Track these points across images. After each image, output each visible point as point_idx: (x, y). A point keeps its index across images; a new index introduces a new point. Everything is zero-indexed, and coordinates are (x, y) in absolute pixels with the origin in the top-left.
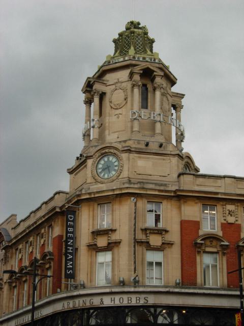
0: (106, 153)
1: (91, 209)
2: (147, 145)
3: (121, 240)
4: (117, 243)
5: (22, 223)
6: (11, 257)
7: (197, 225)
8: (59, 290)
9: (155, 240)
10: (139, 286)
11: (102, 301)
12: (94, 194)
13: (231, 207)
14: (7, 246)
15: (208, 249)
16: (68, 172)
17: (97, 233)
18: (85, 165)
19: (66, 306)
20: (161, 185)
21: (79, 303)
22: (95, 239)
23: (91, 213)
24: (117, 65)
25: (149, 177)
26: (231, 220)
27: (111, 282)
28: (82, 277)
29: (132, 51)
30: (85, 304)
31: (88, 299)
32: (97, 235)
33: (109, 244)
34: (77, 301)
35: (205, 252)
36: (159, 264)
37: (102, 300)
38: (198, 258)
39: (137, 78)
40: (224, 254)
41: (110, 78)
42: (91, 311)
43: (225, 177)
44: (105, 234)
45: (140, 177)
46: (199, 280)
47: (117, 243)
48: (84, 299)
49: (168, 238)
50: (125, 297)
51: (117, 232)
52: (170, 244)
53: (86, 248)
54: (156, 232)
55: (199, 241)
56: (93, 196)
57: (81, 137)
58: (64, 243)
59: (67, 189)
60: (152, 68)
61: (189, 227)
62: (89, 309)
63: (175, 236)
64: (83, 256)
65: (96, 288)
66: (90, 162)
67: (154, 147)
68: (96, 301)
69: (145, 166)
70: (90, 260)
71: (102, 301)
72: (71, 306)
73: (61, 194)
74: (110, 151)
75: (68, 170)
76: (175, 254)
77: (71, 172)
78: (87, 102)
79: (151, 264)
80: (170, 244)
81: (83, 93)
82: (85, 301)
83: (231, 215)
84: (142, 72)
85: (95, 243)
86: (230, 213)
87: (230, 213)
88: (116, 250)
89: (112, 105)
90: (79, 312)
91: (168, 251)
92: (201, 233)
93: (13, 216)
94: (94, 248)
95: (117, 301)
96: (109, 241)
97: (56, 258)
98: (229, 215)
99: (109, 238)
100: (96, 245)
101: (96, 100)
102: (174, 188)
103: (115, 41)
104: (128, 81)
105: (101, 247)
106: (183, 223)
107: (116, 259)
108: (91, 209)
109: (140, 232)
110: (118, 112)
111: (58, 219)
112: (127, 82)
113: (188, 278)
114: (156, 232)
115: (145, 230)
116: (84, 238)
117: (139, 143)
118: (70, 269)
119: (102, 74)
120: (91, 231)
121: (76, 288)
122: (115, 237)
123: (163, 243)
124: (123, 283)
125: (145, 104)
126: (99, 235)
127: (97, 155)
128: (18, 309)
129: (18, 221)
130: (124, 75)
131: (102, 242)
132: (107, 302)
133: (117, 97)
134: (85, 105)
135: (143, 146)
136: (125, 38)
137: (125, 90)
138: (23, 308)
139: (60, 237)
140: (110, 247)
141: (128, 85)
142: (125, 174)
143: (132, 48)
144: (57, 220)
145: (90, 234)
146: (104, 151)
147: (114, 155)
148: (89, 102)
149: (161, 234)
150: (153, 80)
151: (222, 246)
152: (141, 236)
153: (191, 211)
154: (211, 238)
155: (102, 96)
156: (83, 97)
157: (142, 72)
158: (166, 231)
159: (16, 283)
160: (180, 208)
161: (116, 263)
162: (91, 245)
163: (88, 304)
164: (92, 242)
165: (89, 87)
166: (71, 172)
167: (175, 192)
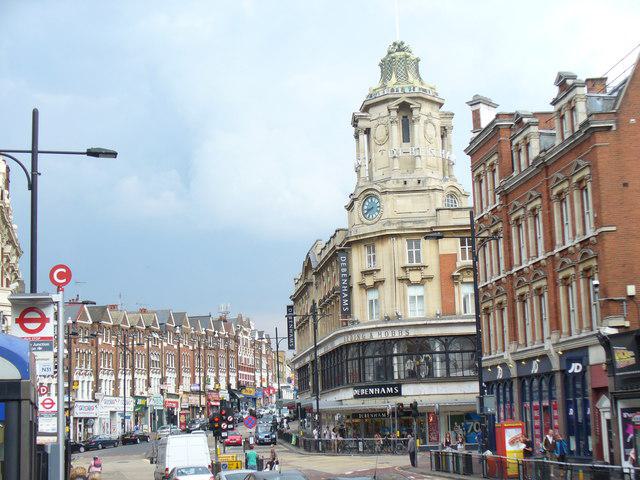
2: (405, 183)
4: (382, 282)
9: (415, 276)
10: (400, 321)
15: (465, 280)
17: (365, 273)
20: (420, 222)
21: (355, 338)
25: (409, 215)
28: (357, 314)
29: (394, 80)
36: (421, 297)
41: (374, 112)
46: (459, 308)
47: (382, 282)
49: (427, 272)
50: (390, 332)
52: (430, 278)
55: (455, 274)
59: (346, 226)
63: (433, 270)
64: (356, 291)
66: (356, 203)
67: (412, 185)
68: (367, 337)
76: (433, 287)
79: (413, 298)
80: (430, 278)
88: (381, 288)
95: (383, 335)
102: (429, 225)
109: (401, 271)
113: (448, 308)
115: (404, 268)
116: (356, 279)
117: (398, 182)
118: (345, 307)
119: (366, 108)
121: (353, 323)
122: (379, 276)
124: (388, 319)
125: (406, 137)
127: (363, 196)
130: (382, 110)
131: (369, 281)
132: (376, 336)
133: (379, 133)
137: (386, 125)
143: (394, 75)
147: (376, 197)
152: (401, 274)
158: (425, 267)
165: (355, 122)
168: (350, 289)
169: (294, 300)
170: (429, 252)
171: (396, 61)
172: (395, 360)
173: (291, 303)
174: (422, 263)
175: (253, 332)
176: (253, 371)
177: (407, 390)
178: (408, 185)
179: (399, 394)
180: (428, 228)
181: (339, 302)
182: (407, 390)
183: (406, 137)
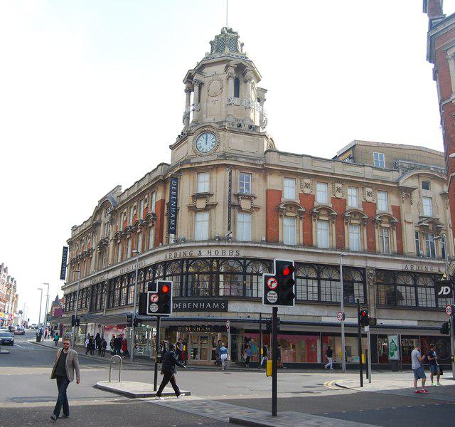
2: (240, 126)
4: (214, 206)
7: (280, 193)
9: (245, 204)
13: (307, 181)
15: (288, 214)
17: (197, 196)
24: (215, 60)
26: (307, 191)
27: (206, 237)
28: (182, 232)
29: (227, 50)
31: (188, 251)
35: (285, 216)
38: (280, 220)
39: (232, 70)
40: (301, 218)
42: (190, 261)
43: (303, 156)
45: (234, 152)
47: (214, 206)
49: (256, 202)
50: (220, 250)
51: (214, 196)
52: (258, 209)
57: (182, 118)
58: (166, 206)
59: (169, 163)
60: (245, 64)
61: (273, 196)
62: (189, 259)
63: (261, 201)
64: (183, 216)
66: (191, 138)
68: (195, 253)
69: (237, 143)
72: (173, 256)
76: (260, 216)
77: (172, 147)
80: (258, 209)
86: (307, 186)
87: (307, 186)
91: (256, 214)
92: (283, 200)
93: (119, 187)
94: (193, 209)
97: (159, 218)
101: (196, 88)
102: (261, 163)
103: (211, 43)
106: (268, 191)
107: (213, 218)
108: (192, 177)
110: (214, 99)
115: (237, 196)
116: (185, 199)
119: (201, 68)
122: (212, 200)
123: (252, 207)
125: (237, 94)
127: (198, 132)
128: (143, 251)
129: (123, 191)
130: (220, 69)
131: (201, 204)
132: (205, 253)
133: (215, 86)
135: (235, 127)
137: (221, 81)
138: (128, 259)
139: (163, 201)
140: (208, 208)
141: (224, 77)
142: (221, 149)
147: (212, 133)
148: (188, 91)
149: (250, 199)
150: (244, 74)
151: (299, 212)
152: (234, 200)
153: (274, 182)
154: (291, 205)
155: (201, 85)
156: (184, 86)
157: (236, 66)
158: (255, 198)
159: (141, 229)
160: (265, 179)
161: (213, 222)
163: (188, 256)
164: (191, 204)
165: (189, 78)
166: (172, 147)
167: (262, 165)
168: (177, 210)
169: (68, 243)
170: (258, 187)
171: (226, 41)
172: (221, 277)
173: (68, 246)
174: (250, 192)
175: (9, 277)
176: (5, 302)
177: (233, 306)
178: (243, 128)
179: (226, 310)
180: (260, 165)
181: (167, 218)
182: (233, 306)
183: (237, 94)
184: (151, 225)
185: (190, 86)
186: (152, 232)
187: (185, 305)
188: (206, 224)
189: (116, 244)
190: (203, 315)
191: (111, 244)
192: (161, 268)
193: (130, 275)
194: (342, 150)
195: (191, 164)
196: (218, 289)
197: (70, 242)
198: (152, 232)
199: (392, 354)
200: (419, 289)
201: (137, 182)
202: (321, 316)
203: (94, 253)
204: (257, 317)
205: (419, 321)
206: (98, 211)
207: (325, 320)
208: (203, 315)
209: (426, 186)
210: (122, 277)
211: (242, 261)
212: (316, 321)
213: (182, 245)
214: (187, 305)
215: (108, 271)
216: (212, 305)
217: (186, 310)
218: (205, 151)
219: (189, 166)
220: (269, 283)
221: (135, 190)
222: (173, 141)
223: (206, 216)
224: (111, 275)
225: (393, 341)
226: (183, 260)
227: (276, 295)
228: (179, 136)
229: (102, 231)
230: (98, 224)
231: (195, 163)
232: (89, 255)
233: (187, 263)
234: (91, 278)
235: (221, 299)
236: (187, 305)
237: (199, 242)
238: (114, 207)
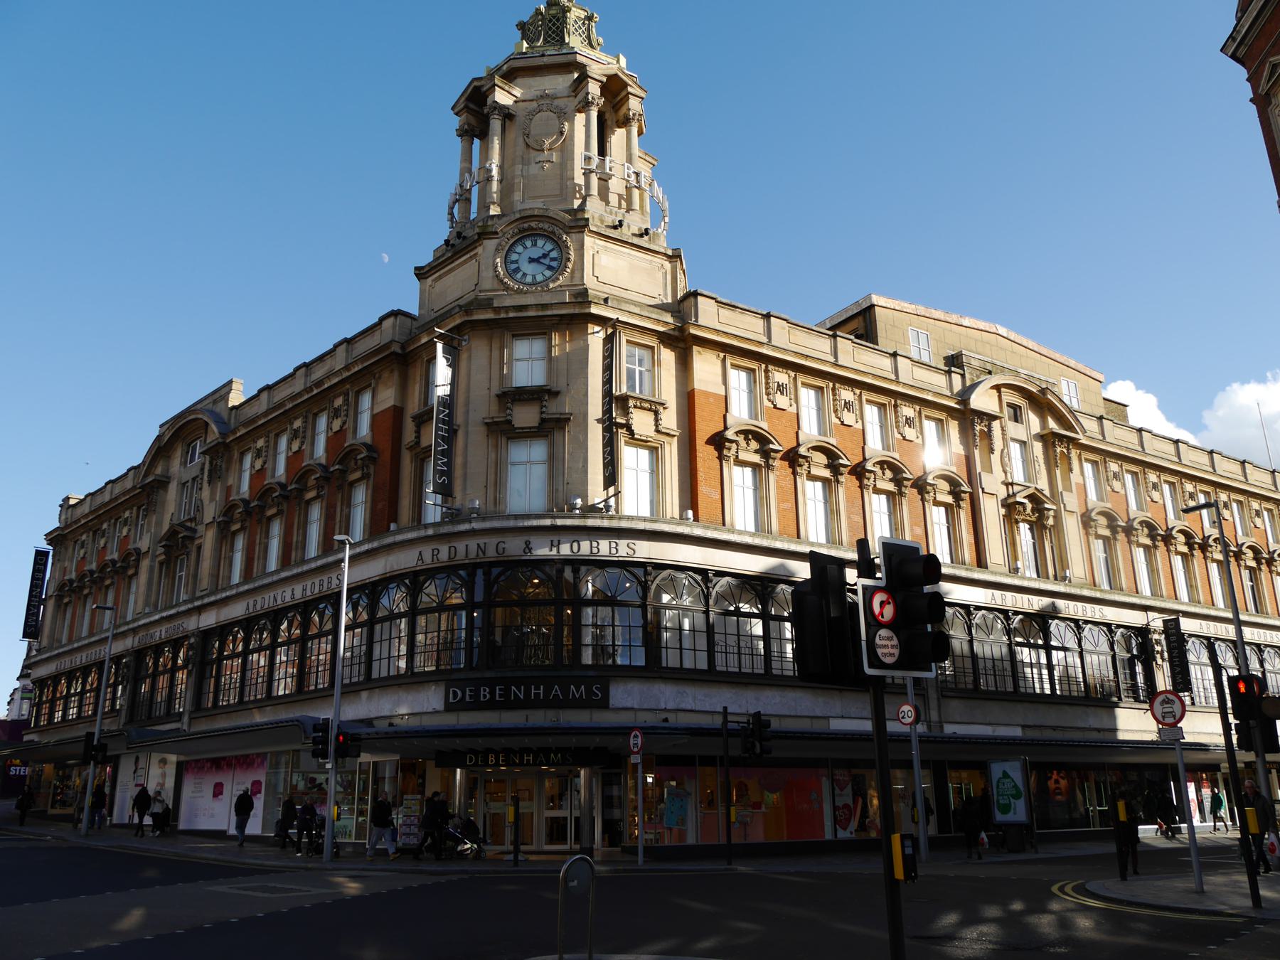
0: (531, 228)
1: (496, 345)
3: (571, 414)
5: (264, 396)
6: (228, 470)
8: (393, 526)
11: (527, 546)
12: (507, 312)
14: (219, 443)
16: (416, 275)
18: (472, 253)
19: (428, 557)
22: (508, 408)
23: (496, 353)
30: (484, 553)
31: (492, 542)
32: (513, 401)
33: (543, 421)
34: (461, 546)
37: (527, 544)
44: (533, 399)
48: (481, 541)
53: (483, 429)
54: (647, 405)
56: (503, 315)
59: (414, 310)
65: (509, 517)
68: (514, 547)
70: (493, 456)
71: (527, 546)
73: (400, 317)
74: (541, 225)
75: (416, 268)
77: (421, 273)
78: (467, 131)
81: (456, 114)
82: (482, 546)
83: (782, 393)
84: (604, 79)
85: (509, 418)
88: (557, 435)
89: (530, 141)
90: (461, 572)
96: (544, 416)
97: (386, 456)
98: (779, 392)
99: (544, 409)
100: (509, 422)
104: (569, 97)
105: (522, 428)
108: (496, 345)
111: (392, 371)
112: (566, 99)
114: (647, 405)
120: (496, 390)
122: (553, 408)
126: (520, 400)
131: (525, 416)
134: (459, 139)
136: (550, 21)
139: (397, 413)
144: (386, 375)
145: (494, 401)
146: (526, 225)
147: (549, 237)
148: (467, 133)
157: (604, 79)
162: (497, 423)
163: (491, 553)
166: (421, 273)
169: (50, 542)
177: (624, 695)
179: (604, 704)
182: (624, 695)
184: (357, 475)
185: (473, 120)
186: (360, 496)
187: (485, 693)
188: (540, 472)
189: (225, 535)
190: (539, 718)
191: (208, 539)
192: (396, 600)
193: (276, 616)
194: (845, 310)
195: (497, 310)
196: (578, 645)
197: (55, 538)
198: (360, 496)
199: (1006, 809)
200: (1054, 652)
201: (305, 365)
202: (827, 718)
203: (145, 564)
204: (718, 721)
205: (1024, 727)
206: (160, 450)
207: (837, 725)
208: (539, 718)
209: (1017, 416)
210: (248, 624)
211: (639, 572)
212: (818, 726)
213: (476, 525)
214: (492, 693)
215: (200, 610)
216: (565, 691)
217: (491, 705)
218: (529, 279)
219: (489, 315)
220: (877, 609)
221: (298, 385)
222: (426, 259)
223: (538, 450)
224: (209, 620)
225: (1005, 775)
226: (472, 567)
227: (895, 642)
228: (447, 242)
229: (172, 505)
230: (162, 483)
231: (507, 309)
232: (125, 569)
233: (487, 574)
234: (135, 631)
235: (591, 673)
236: (492, 693)
237: (517, 517)
238: (223, 435)
